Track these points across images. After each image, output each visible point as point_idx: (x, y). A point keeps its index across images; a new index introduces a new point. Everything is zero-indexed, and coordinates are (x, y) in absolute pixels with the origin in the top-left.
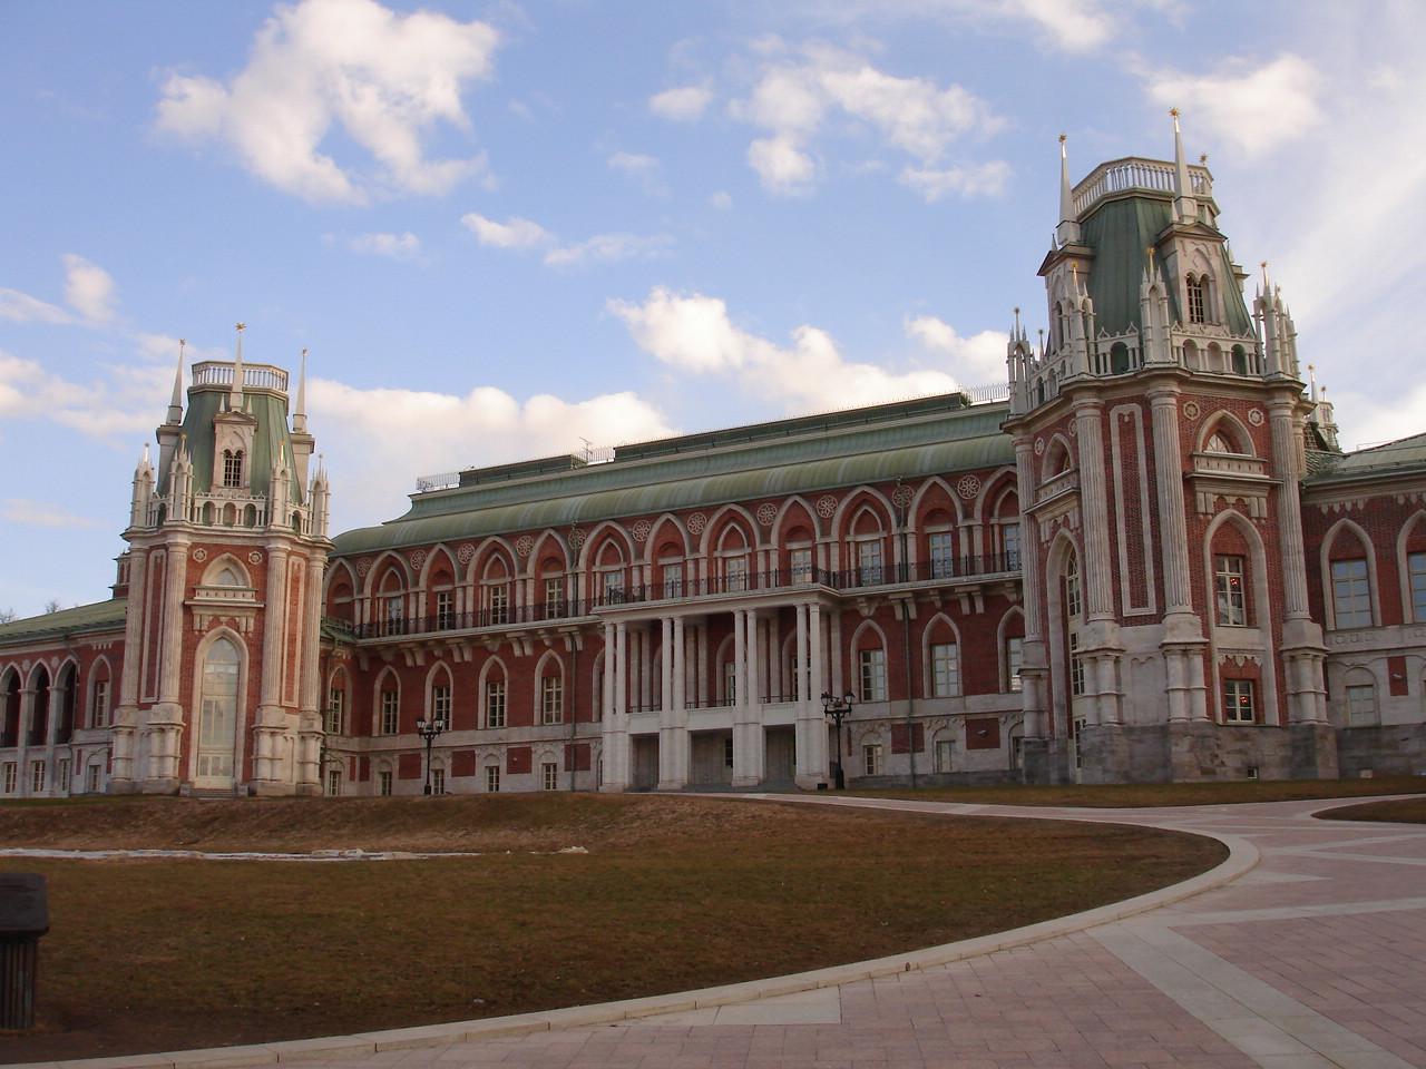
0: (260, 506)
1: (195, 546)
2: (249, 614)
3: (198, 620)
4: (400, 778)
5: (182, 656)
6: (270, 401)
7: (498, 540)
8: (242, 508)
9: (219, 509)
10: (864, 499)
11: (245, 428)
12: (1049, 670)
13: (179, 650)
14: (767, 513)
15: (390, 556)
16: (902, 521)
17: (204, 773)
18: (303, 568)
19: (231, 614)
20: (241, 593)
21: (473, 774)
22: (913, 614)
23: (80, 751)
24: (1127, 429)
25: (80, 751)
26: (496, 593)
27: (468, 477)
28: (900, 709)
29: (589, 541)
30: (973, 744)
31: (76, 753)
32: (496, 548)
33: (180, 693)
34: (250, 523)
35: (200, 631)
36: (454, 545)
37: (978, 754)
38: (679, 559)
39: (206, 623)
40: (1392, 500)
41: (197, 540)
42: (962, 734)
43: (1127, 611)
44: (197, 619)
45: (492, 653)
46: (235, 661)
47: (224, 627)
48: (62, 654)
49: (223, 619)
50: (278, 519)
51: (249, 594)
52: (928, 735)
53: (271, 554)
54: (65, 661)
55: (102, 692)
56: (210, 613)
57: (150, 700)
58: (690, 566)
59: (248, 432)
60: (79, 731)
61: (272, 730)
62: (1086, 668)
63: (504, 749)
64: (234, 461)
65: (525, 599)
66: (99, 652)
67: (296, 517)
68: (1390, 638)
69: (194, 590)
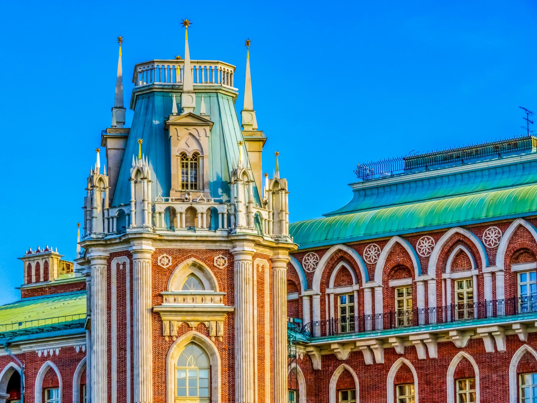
0: (223, 209)
1: (160, 251)
2: (218, 318)
3: (168, 326)
5: (154, 363)
6: (220, 99)
8: (205, 211)
9: (181, 213)
11: (201, 129)
13: (150, 356)
15: (340, 250)
20: (208, 298)
26: (460, 286)
27: (413, 163)
32: (459, 240)
34: (213, 226)
35: (170, 337)
36: (412, 238)
39: (176, 329)
44: (166, 324)
46: (205, 364)
47: (194, 332)
49: (193, 324)
50: (242, 220)
51: (217, 298)
53: (236, 258)
55: (49, 398)
56: (179, 318)
64: (192, 162)
67: (258, 219)
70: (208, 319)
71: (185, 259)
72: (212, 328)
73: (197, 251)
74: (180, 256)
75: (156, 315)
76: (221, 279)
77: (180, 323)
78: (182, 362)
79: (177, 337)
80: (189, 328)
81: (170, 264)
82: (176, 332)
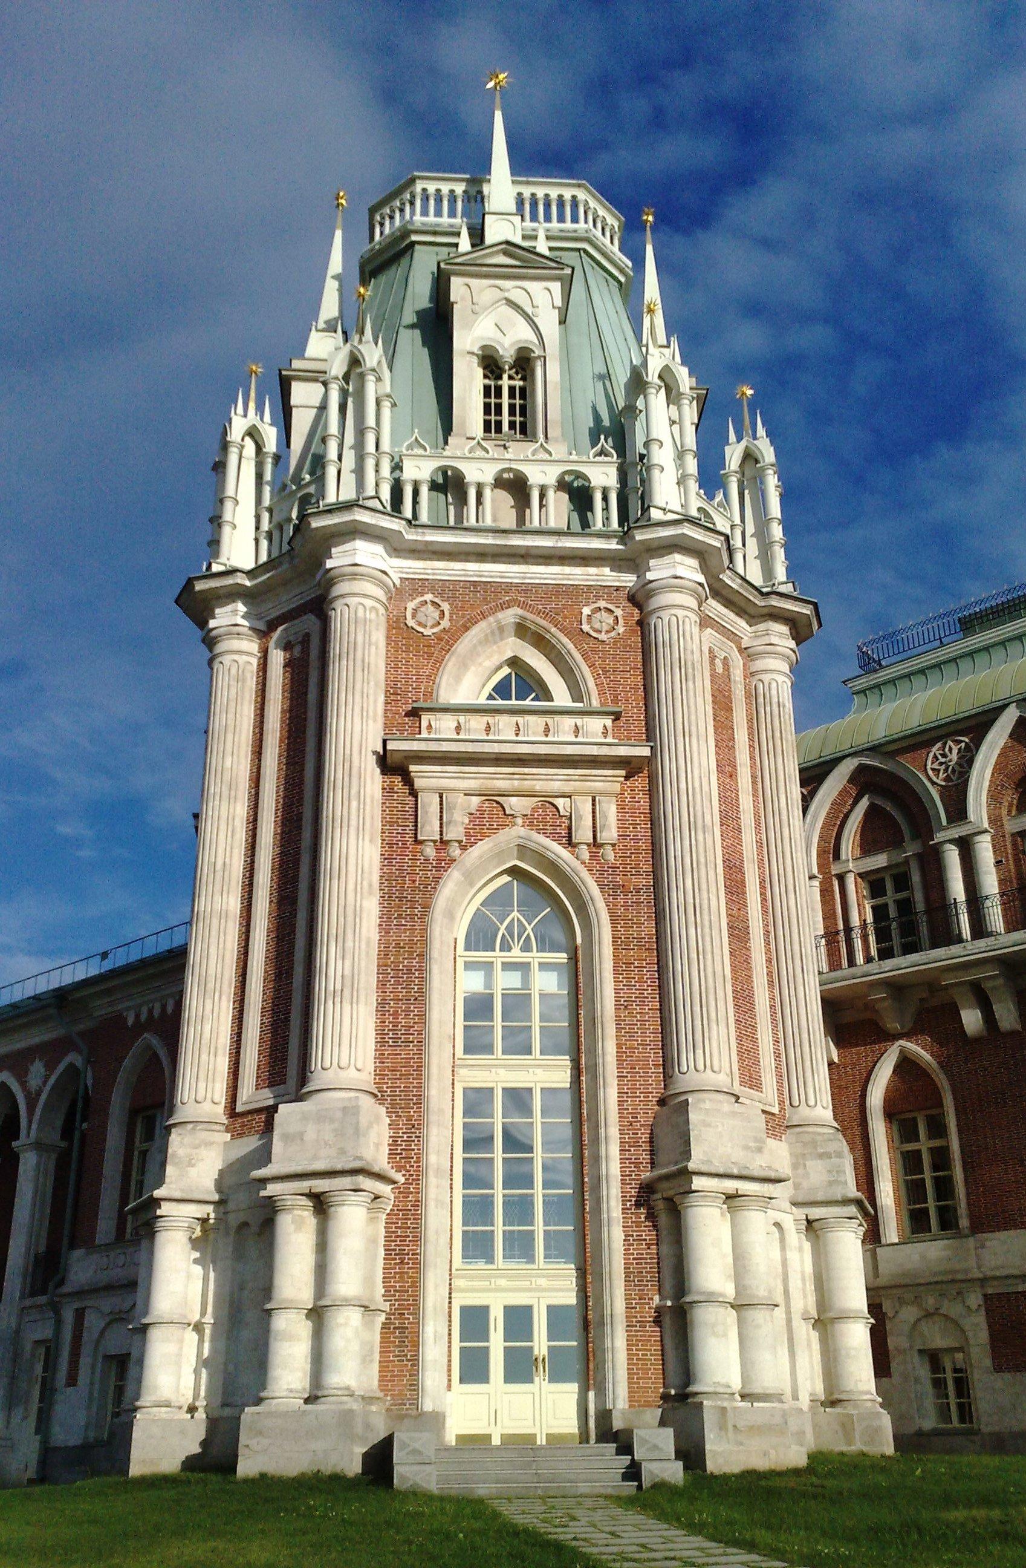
0: (603, 475)
4: (998, 1368)
5: (385, 928)
13: (371, 907)
17: (474, 1369)
18: (737, 674)
19: (539, 786)
23: (80, 1315)
25: (80, 1315)
31: (68, 1316)
33: (380, 1058)
44: (429, 804)
48: (51, 1052)
49: (514, 804)
54: (61, 1067)
59: (543, 296)
60: (78, 1253)
61: (730, 1185)
66: (140, 1028)
69: (414, 713)
70: (567, 787)
71: (493, 611)
72: (580, 818)
73: (527, 589)
74: (471, 603)
75: (393, 766)
76: (605, 671)
77: (476, 800)
78: (481, 936)
79: (464, 848)
80: (507, 817)
81: (445, 623)
82: (462, 830)
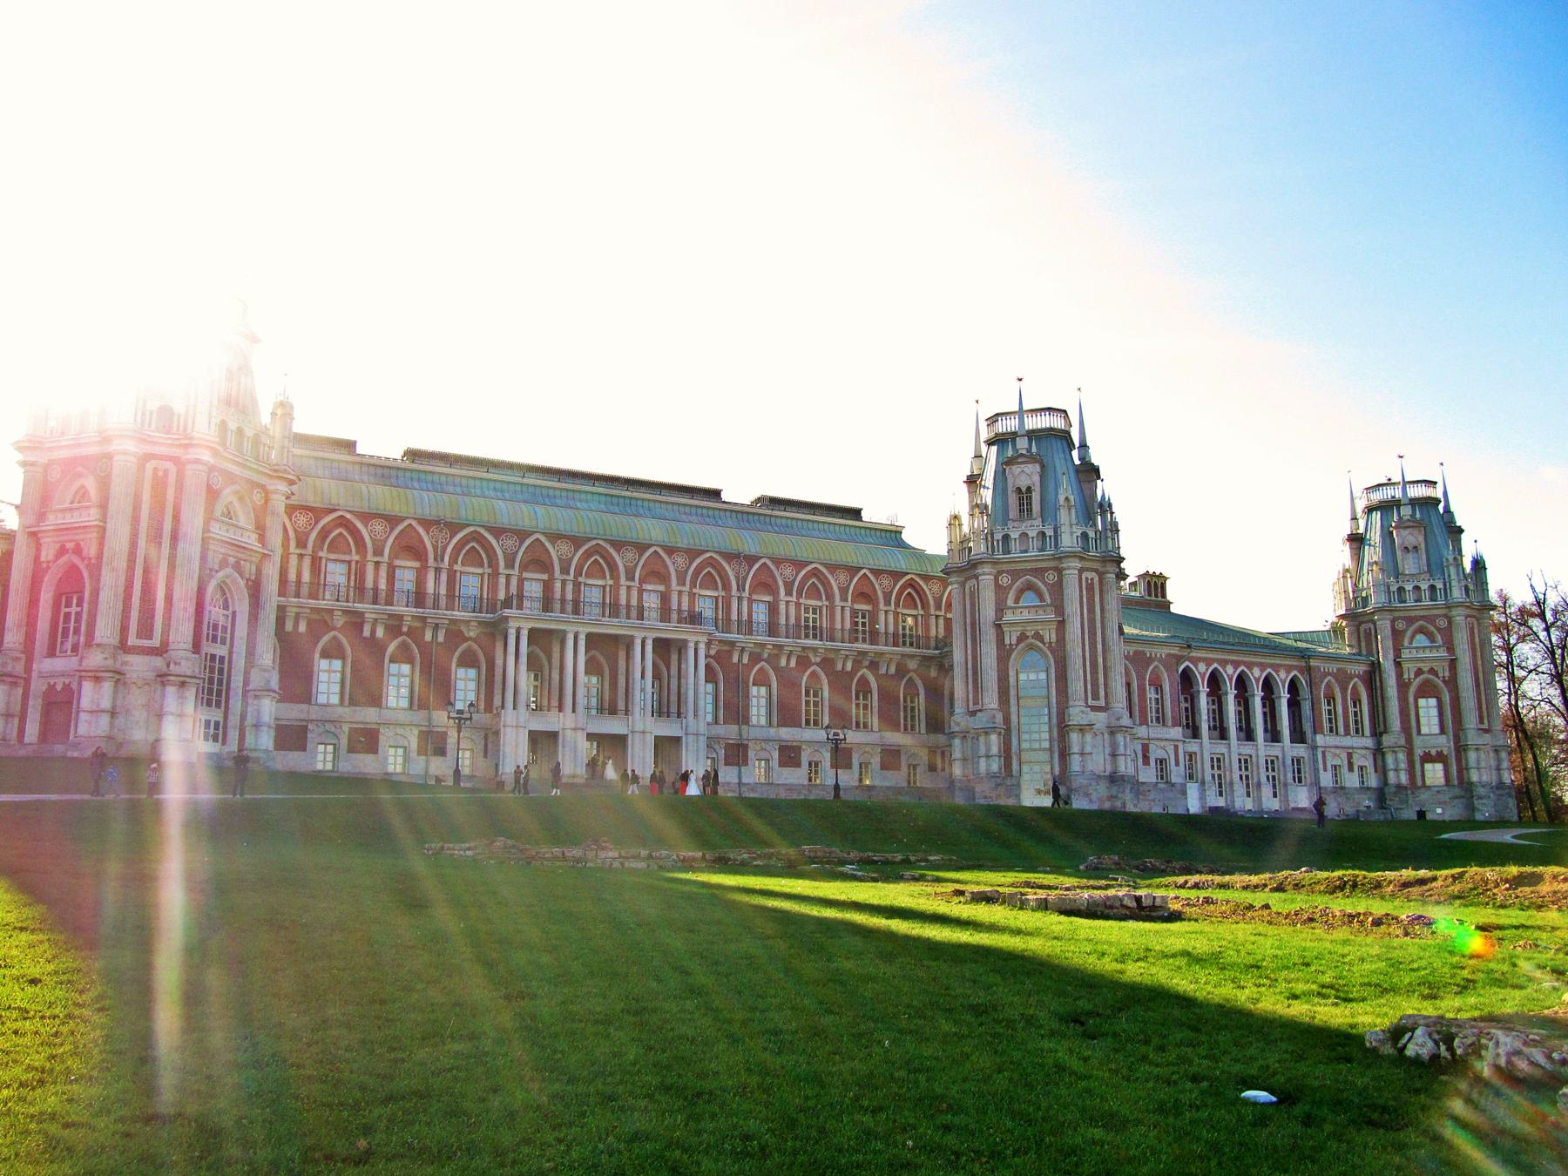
7: (348, 516)
10: (710, 562)
12: (1008, 730)
14: (630, 555)
16: (741, 588)
21: (304, 750)
22: (745, 660)
24: (1090, 588)
28: (730, 731)
29: (455, 541)
30: (782, 764)
37: (786, 771)
38: (545, 577)
40: (1143, 653)
41: (149, 449)
42: (776, 755)
43: (1090, 702)
45: (334, 629)
47: (229, 570)
52: (751, 754)
57: (145, 643)
58: (558, 585)
62: (1074, 737)
63: (346, 728)
65: (376, 582)
68: (1142, 731)
